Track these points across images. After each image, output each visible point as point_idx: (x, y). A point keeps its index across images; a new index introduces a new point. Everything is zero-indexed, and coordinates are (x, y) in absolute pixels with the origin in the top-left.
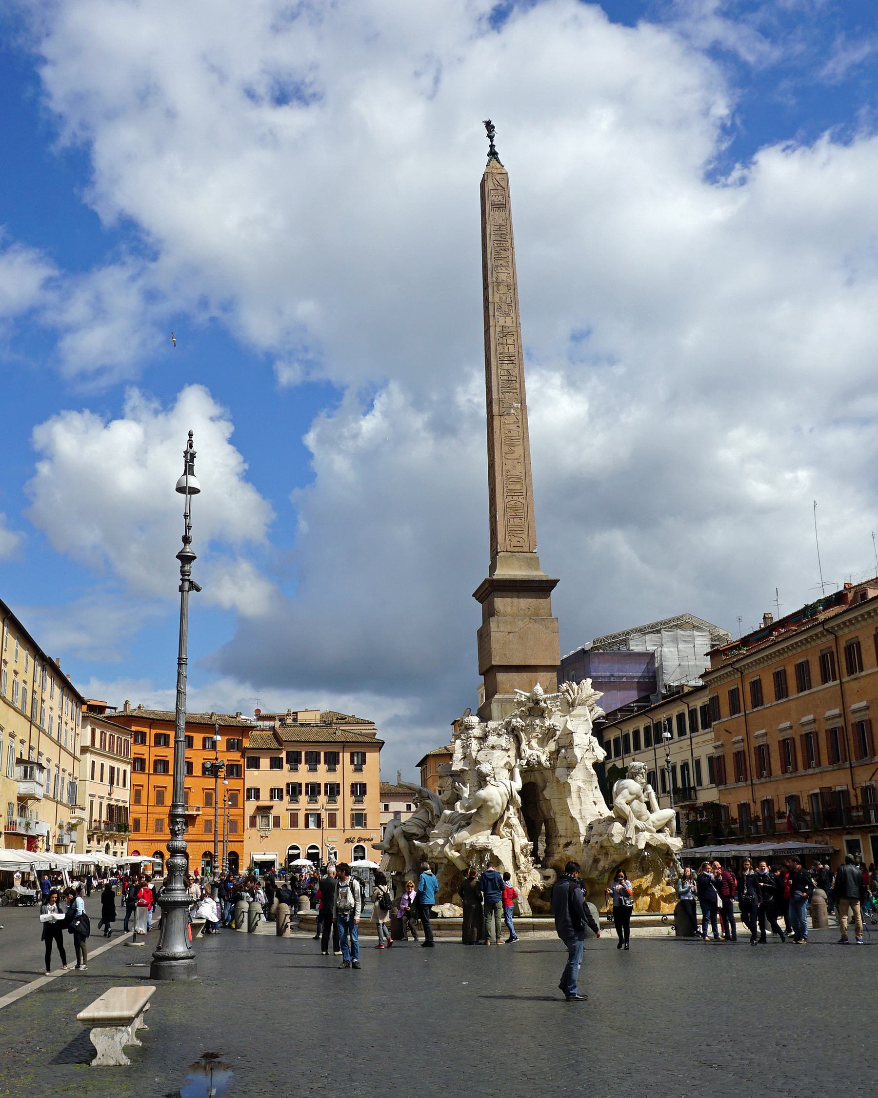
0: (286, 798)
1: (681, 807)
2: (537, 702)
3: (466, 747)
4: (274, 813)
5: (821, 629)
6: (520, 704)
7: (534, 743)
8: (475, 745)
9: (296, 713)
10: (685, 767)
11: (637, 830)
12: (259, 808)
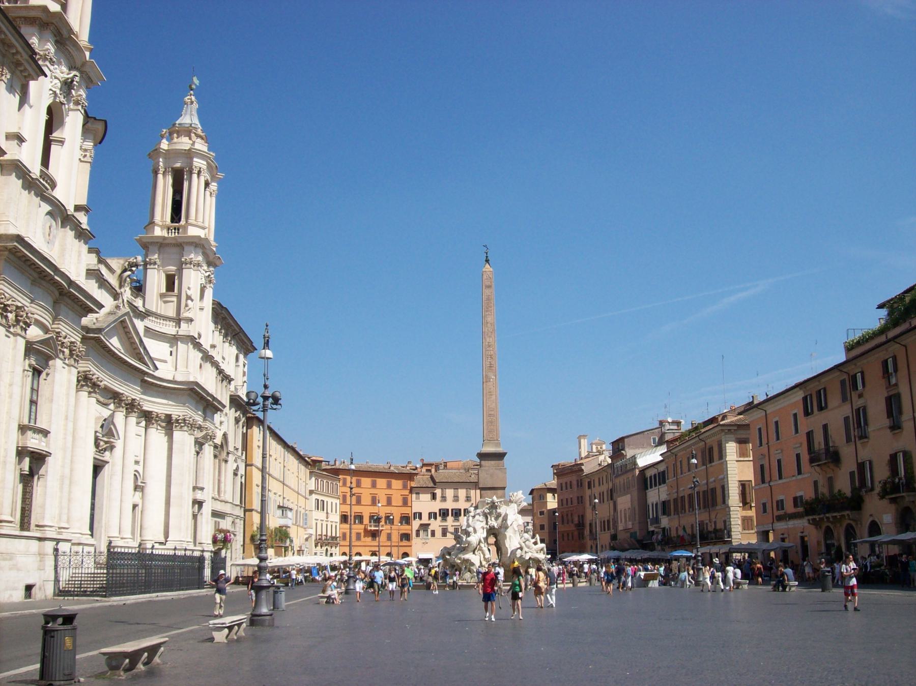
0: (439, 518)
1: (655, 527)
2: (494, 503)
3: (468, 520)
4: (431, 528)
5: (697, 439)
6: (488, 504)
7: (493, 519)
8: (471, 518)
9: (446, 463)
10: (657, 504)
11: (526, 552)
12: (421, 525)
